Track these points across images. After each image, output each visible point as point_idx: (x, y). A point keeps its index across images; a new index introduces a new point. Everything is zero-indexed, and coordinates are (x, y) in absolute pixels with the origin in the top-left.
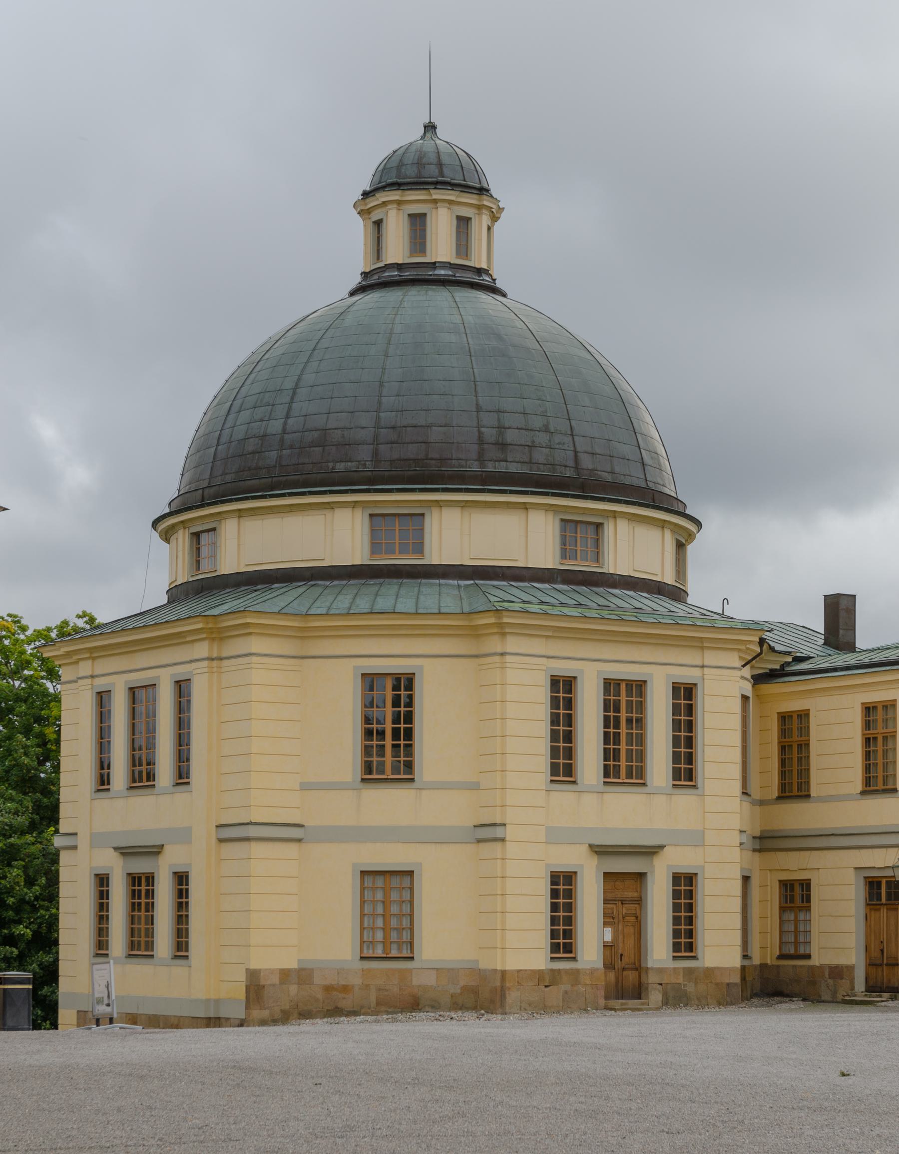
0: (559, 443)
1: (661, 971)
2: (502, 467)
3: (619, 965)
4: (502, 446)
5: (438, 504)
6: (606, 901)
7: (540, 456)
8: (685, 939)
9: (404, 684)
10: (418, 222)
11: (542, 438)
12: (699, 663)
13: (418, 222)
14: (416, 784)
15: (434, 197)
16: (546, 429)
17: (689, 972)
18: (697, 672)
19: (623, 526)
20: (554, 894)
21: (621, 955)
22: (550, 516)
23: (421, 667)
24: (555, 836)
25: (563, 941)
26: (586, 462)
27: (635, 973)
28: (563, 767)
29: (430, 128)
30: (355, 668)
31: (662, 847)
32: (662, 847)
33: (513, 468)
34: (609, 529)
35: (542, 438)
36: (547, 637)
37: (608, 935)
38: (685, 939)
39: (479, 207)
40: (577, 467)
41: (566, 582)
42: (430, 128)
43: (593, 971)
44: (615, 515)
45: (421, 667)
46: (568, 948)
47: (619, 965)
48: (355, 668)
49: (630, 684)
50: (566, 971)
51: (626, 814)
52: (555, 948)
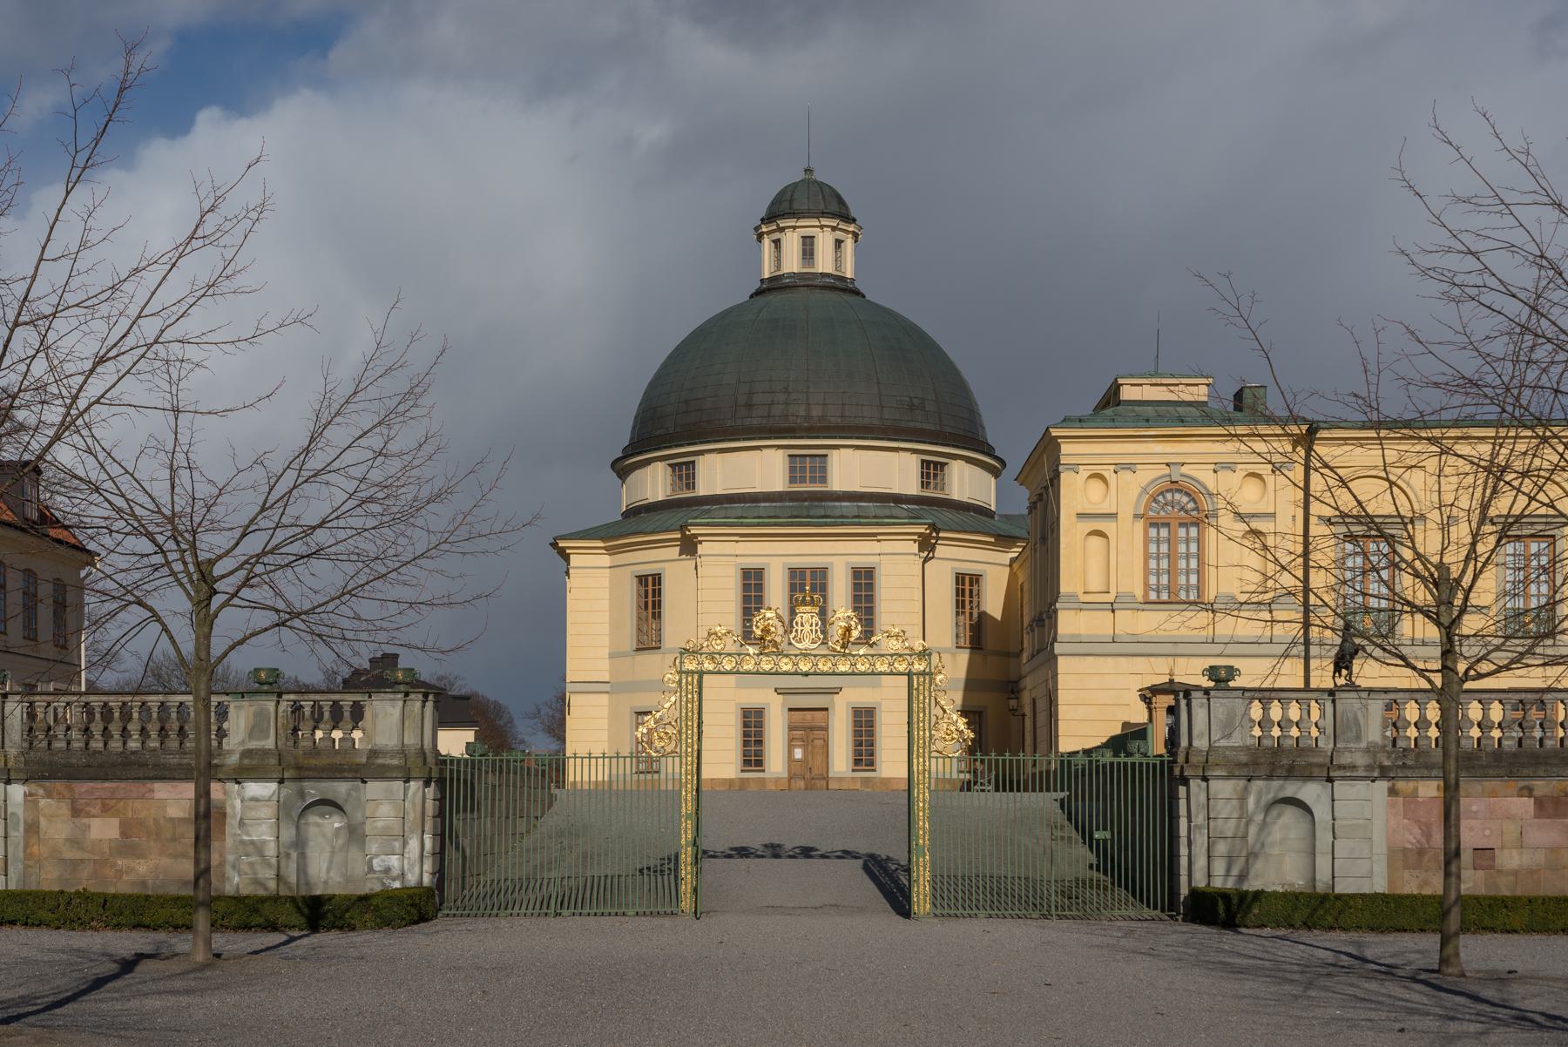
1: (840, 779)
2: (747, 422)
3: (808, 775)
4: (749, 406)
5: (701, 453)
6: (791, 729)
7: (777, 411)
8: (864, 754)
9: (657, 579)
10: (808, 245)
13: (808, 245)
16: (786, 390)
17: (866, 781)
18: (876, 559)
20: (746, 725)
22: (781, 452)
25: (753, 756)
27: (824, 783)
29: (808, 171)
33: (755, 422)
35: (781, 397)
37: (798, 754)
38: (864, 754)
39: (822, 227)
40: (808, 417)
41: (791, 500)
43: (777, 780)
46: (759, 763)
47: (808, 775)
49: (814, 571)
52: (747, 762)
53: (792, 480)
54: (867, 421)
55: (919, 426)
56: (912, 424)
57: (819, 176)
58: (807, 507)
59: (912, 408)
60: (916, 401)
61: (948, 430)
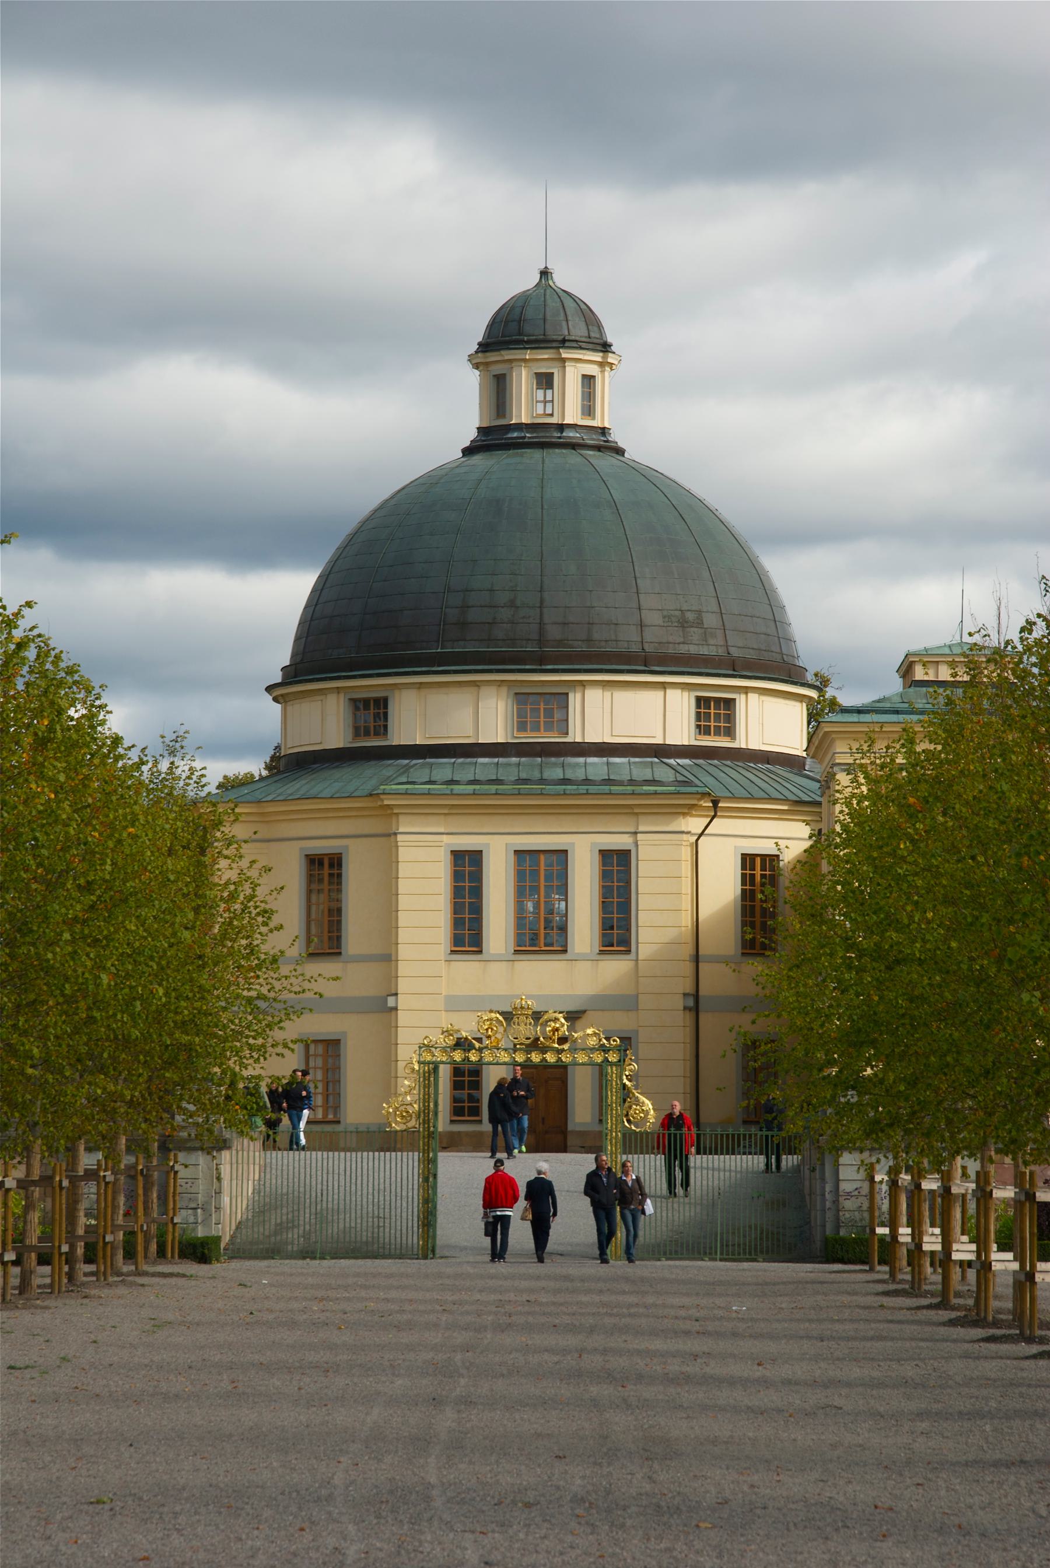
0: (524, 617)
11: (505, 614)
12: (633, 830)
14: (342, 958)
15: (506, 358)
16: (512, 604)
19: (593, 695)
21: (543, 1119)
23: (347, 847)
24: (454, 1004)
26: (554, 632)
28: (467, 935)
29: (545, 273)
30: (301, 849)
31: (584, 1012)
32: (584, 1012)
34: (575, 699)
36: (445, 814)
41: (519, 755)
42: (545, 273)
44: (583, 684)
45: (347, 847)
48: (301, 849)
50: (467, 1134)
51: (544, 982)
53: (522, 727)
54: (622, 647)
55: (693, 649)
56: (683, 649)
57: (561, 280)
58: (542, 766)
59: (683, 624)
60: (690, 616)
61: (735, 652)
